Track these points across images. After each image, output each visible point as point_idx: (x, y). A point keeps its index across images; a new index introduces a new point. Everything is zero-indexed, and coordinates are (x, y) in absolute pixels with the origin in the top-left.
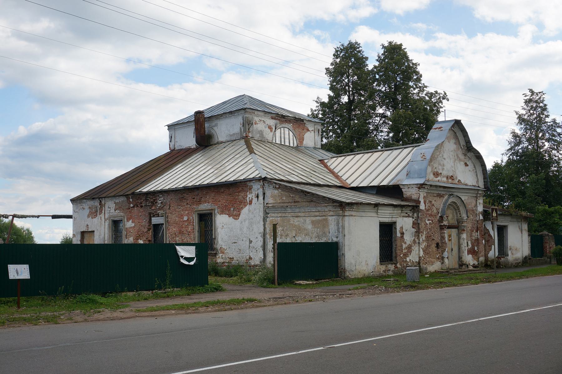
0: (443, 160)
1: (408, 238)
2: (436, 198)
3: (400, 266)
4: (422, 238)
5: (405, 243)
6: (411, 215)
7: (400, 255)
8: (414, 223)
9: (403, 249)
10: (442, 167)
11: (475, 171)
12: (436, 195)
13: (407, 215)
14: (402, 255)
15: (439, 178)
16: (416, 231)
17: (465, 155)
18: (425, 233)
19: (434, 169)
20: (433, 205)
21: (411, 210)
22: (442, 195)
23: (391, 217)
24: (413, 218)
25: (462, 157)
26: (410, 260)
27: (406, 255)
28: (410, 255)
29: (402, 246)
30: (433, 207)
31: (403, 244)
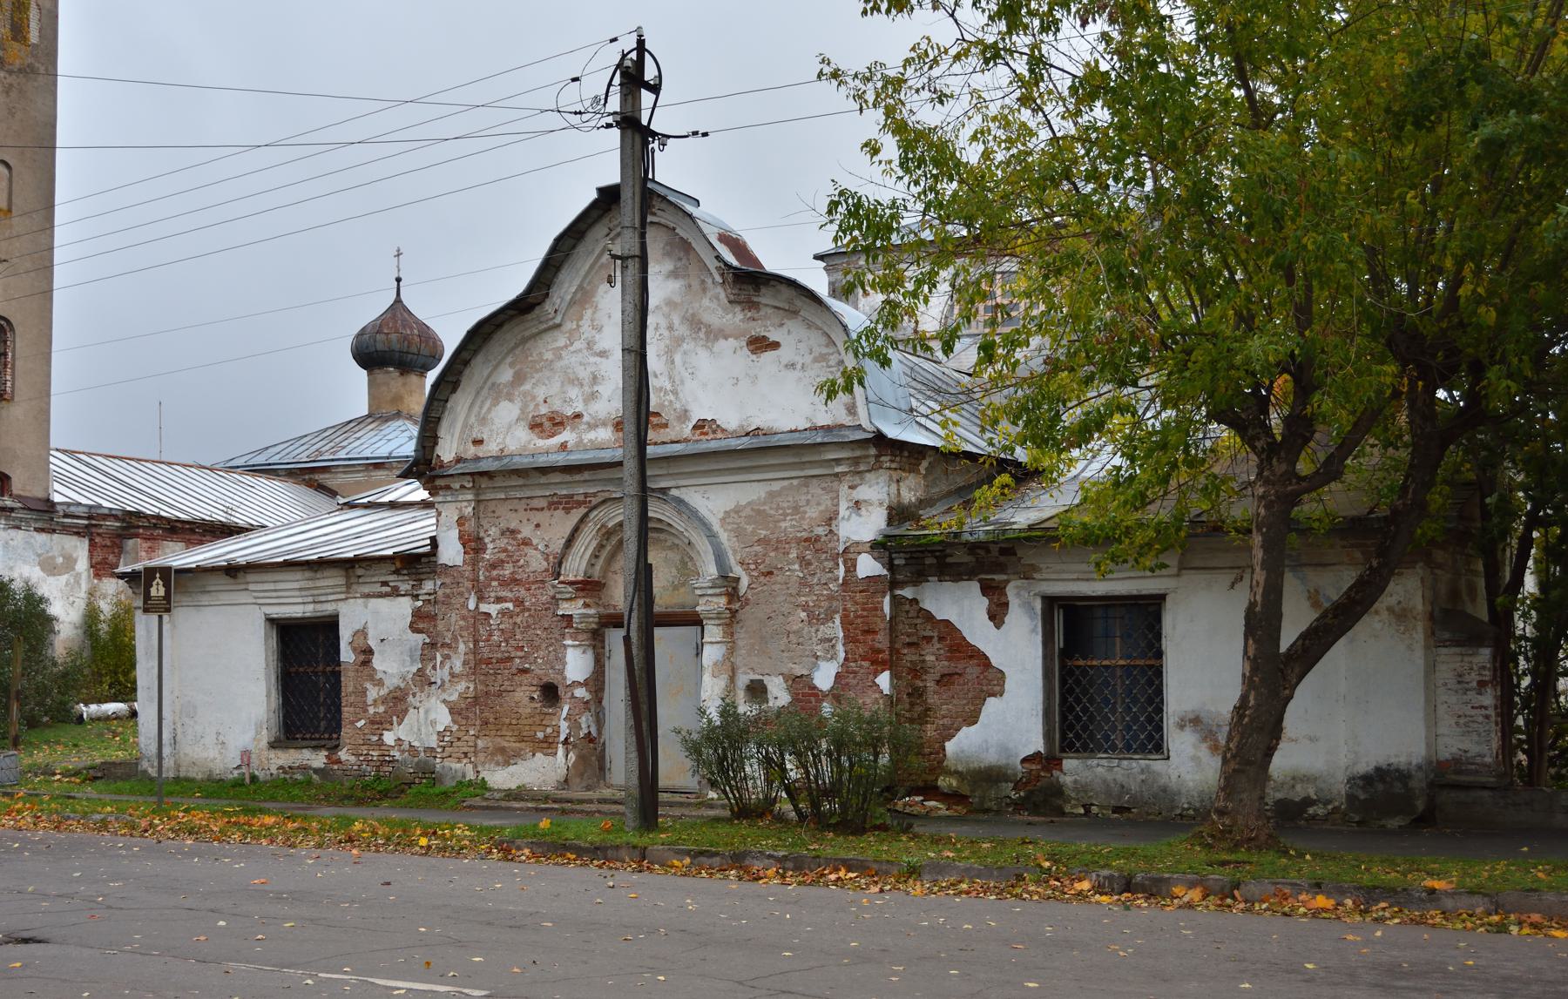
0: (598, 359)
1: (392, 666)
2: (547, 513)
3: (353, 759)
4: (447, 667)
5: (380, 683)
6: (409, 587)
7: (353, 723)
8: (417, 615)
9: (369, 701)
10: (587, 389)
11: (833, 360)
12: (545, 505)
13: (388, 589)
14: (359, 724)
15: (567, 436)
16: (428, 641)
17: (751, 305)
18: (462, 647)
19: (537, 405)
20: (526, 542)
21: (397, 572)
22: (581, 498)
23: (310, 599)
24: (416, 597)
25: (736, 318)
26: (399, 739)
27: (380, 724)
28: (399, 724)
29: (364, 692)
30: (527, 549)
31: (368, 685)
